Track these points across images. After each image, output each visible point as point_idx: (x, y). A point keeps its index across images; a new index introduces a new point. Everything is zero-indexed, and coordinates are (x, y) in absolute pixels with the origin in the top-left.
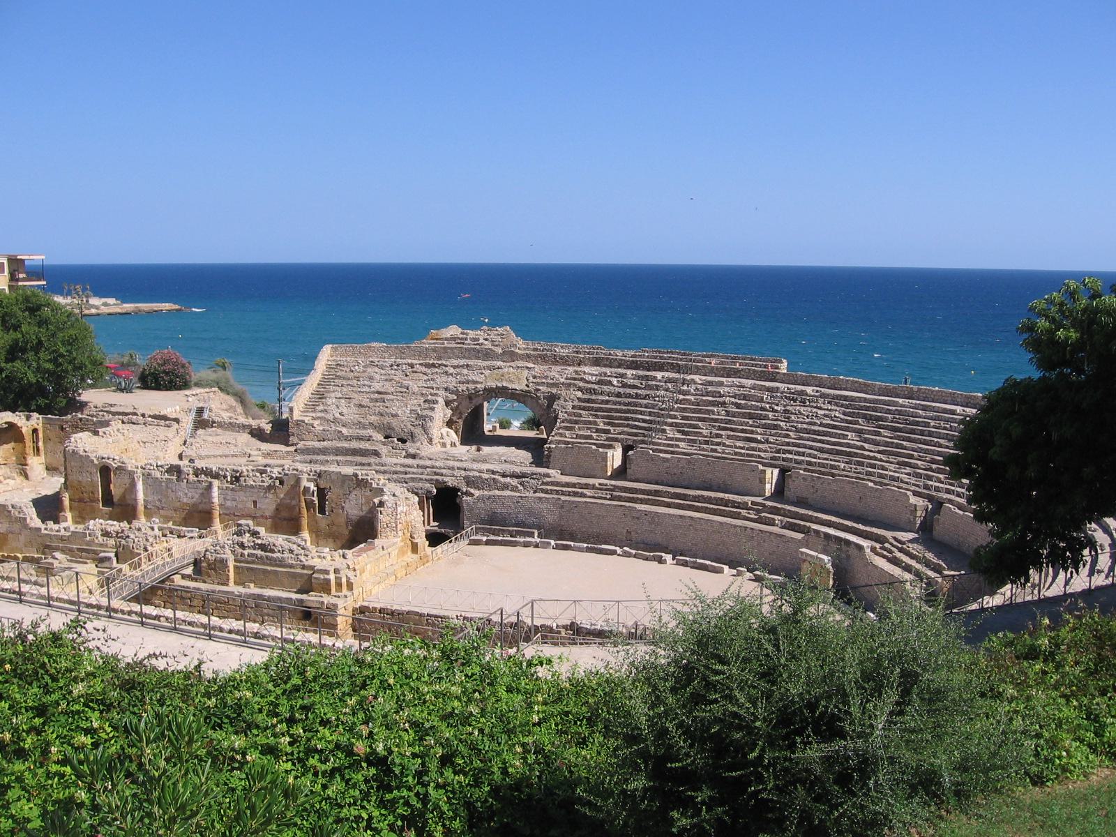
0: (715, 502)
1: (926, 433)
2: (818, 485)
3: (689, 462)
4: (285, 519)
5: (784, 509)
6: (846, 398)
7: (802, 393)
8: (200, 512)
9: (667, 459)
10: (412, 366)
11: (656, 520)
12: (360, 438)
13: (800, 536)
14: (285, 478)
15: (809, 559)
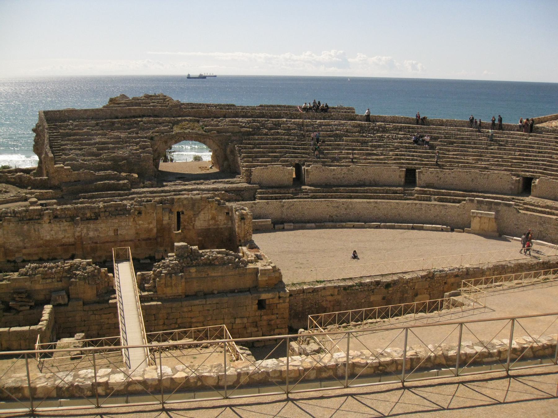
0: (378, 191)
1: (472, 143)
2: (441, 175)
3: (349, 170)
4: (144, 240)
5: (430, 191)
6: (409, 127)
7: (380, 126)
8: (63, 245)
9: (334, 170)
10: (113, 123)
11: (350, 206)
12: (108, 178)
13: (458, 205)
14: (143, 208)
15: (479, 215)
